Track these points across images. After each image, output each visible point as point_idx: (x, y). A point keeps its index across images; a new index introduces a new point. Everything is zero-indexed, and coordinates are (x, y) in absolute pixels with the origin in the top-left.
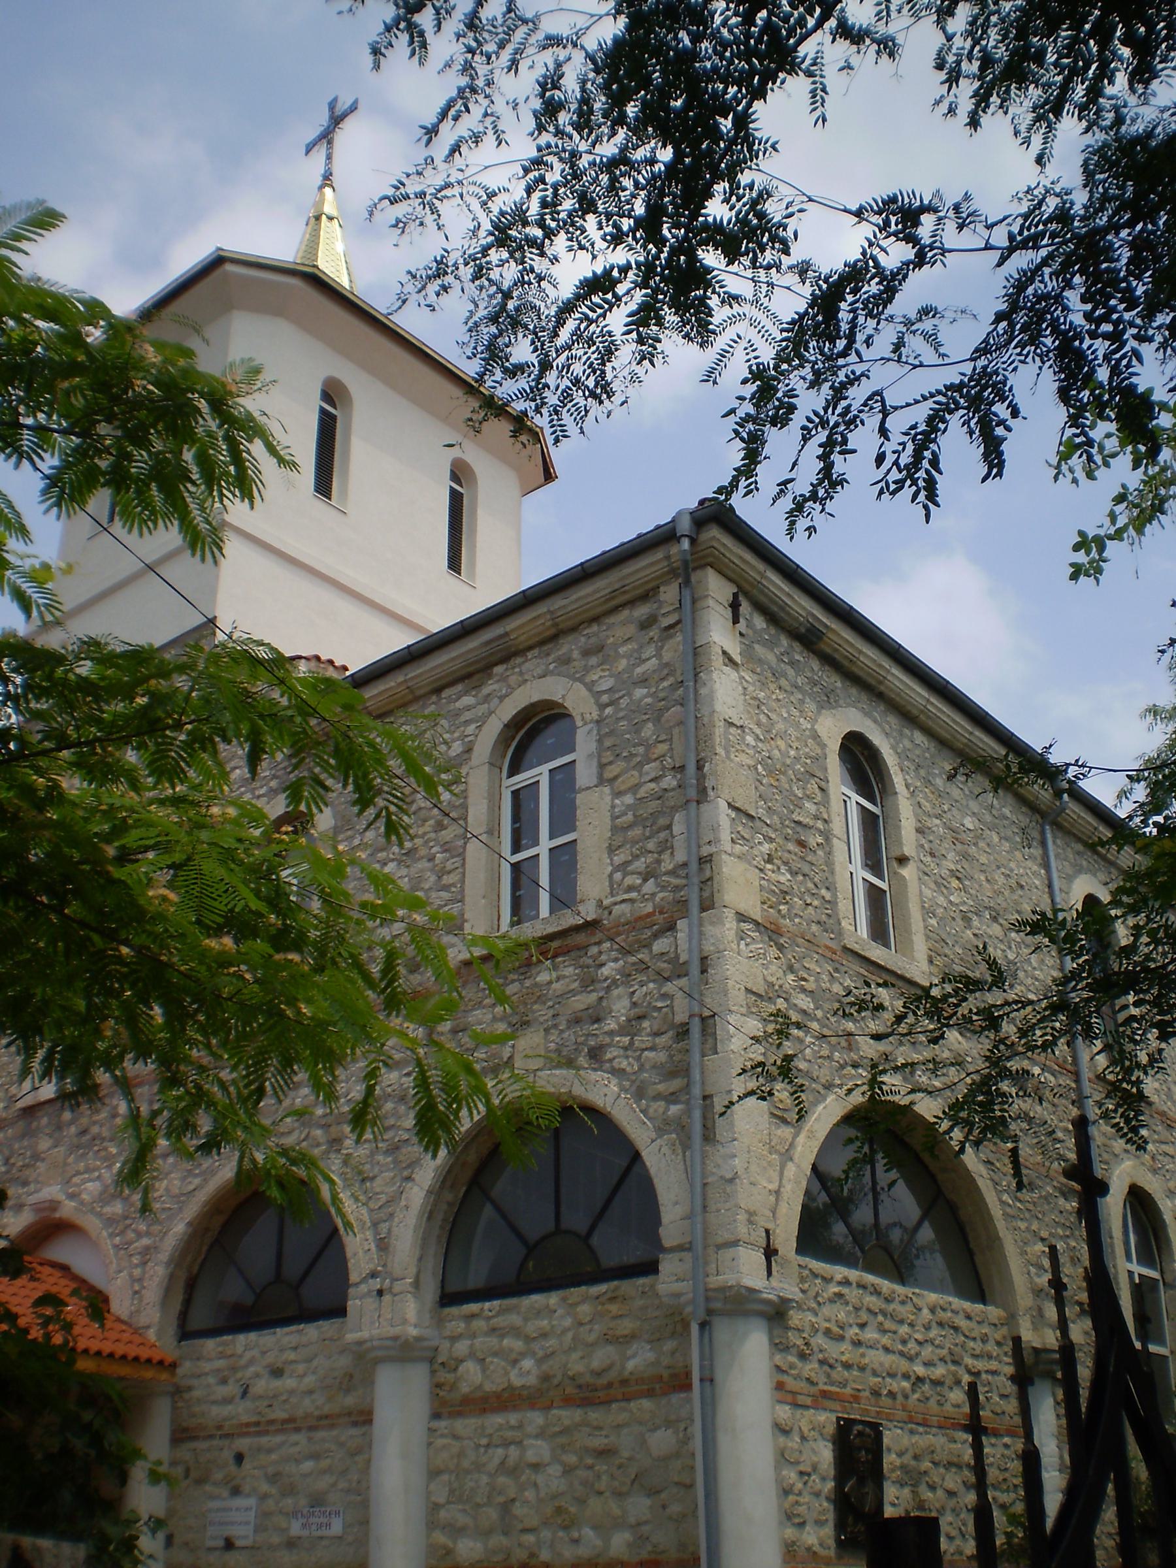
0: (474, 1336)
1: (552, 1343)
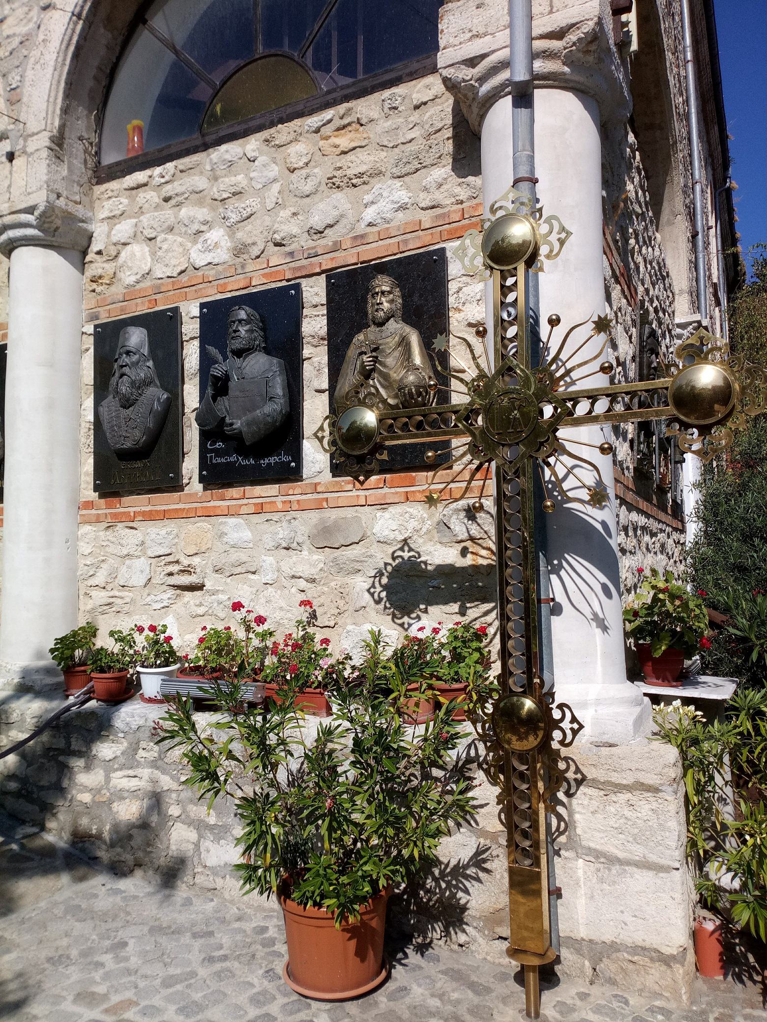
0: (141, 211)
1: (251, 203)
